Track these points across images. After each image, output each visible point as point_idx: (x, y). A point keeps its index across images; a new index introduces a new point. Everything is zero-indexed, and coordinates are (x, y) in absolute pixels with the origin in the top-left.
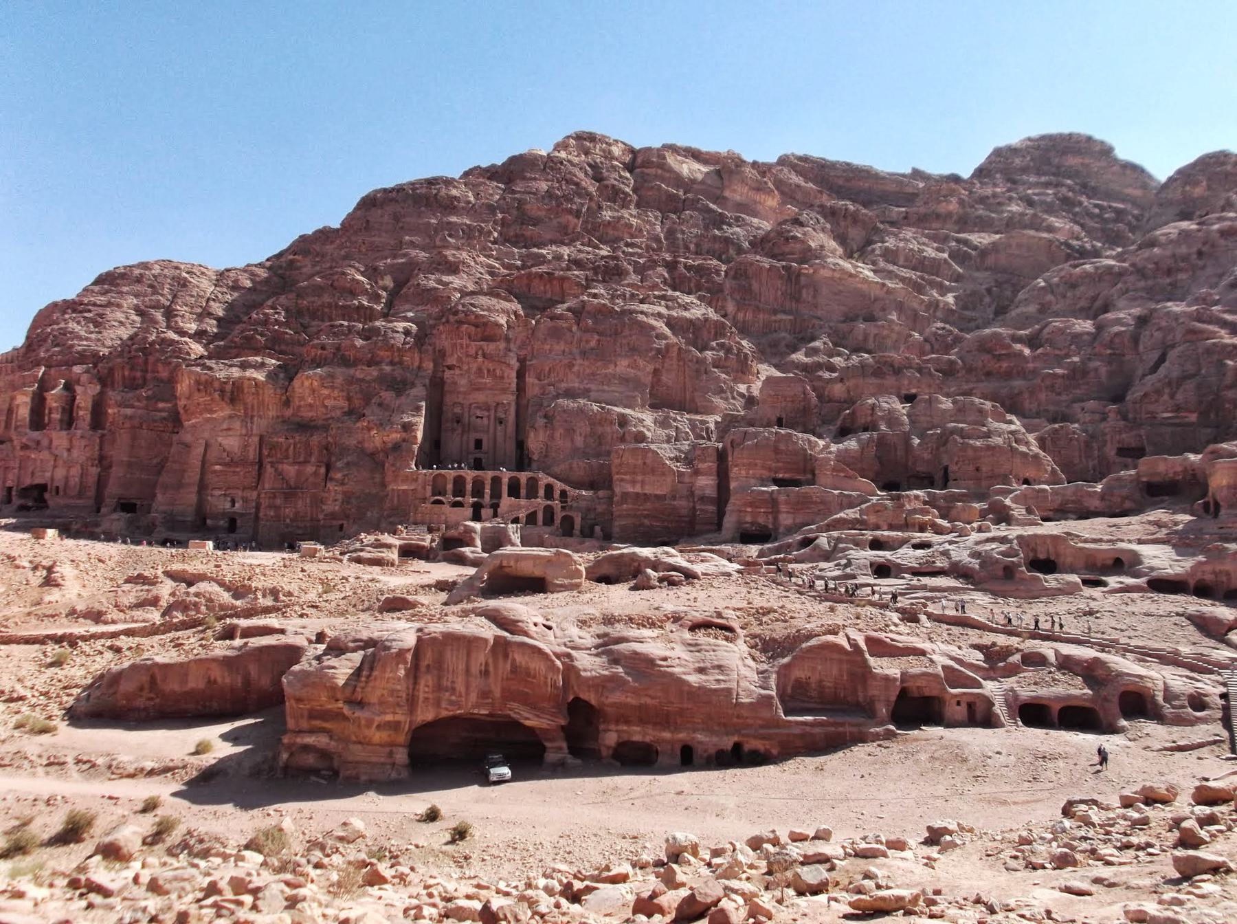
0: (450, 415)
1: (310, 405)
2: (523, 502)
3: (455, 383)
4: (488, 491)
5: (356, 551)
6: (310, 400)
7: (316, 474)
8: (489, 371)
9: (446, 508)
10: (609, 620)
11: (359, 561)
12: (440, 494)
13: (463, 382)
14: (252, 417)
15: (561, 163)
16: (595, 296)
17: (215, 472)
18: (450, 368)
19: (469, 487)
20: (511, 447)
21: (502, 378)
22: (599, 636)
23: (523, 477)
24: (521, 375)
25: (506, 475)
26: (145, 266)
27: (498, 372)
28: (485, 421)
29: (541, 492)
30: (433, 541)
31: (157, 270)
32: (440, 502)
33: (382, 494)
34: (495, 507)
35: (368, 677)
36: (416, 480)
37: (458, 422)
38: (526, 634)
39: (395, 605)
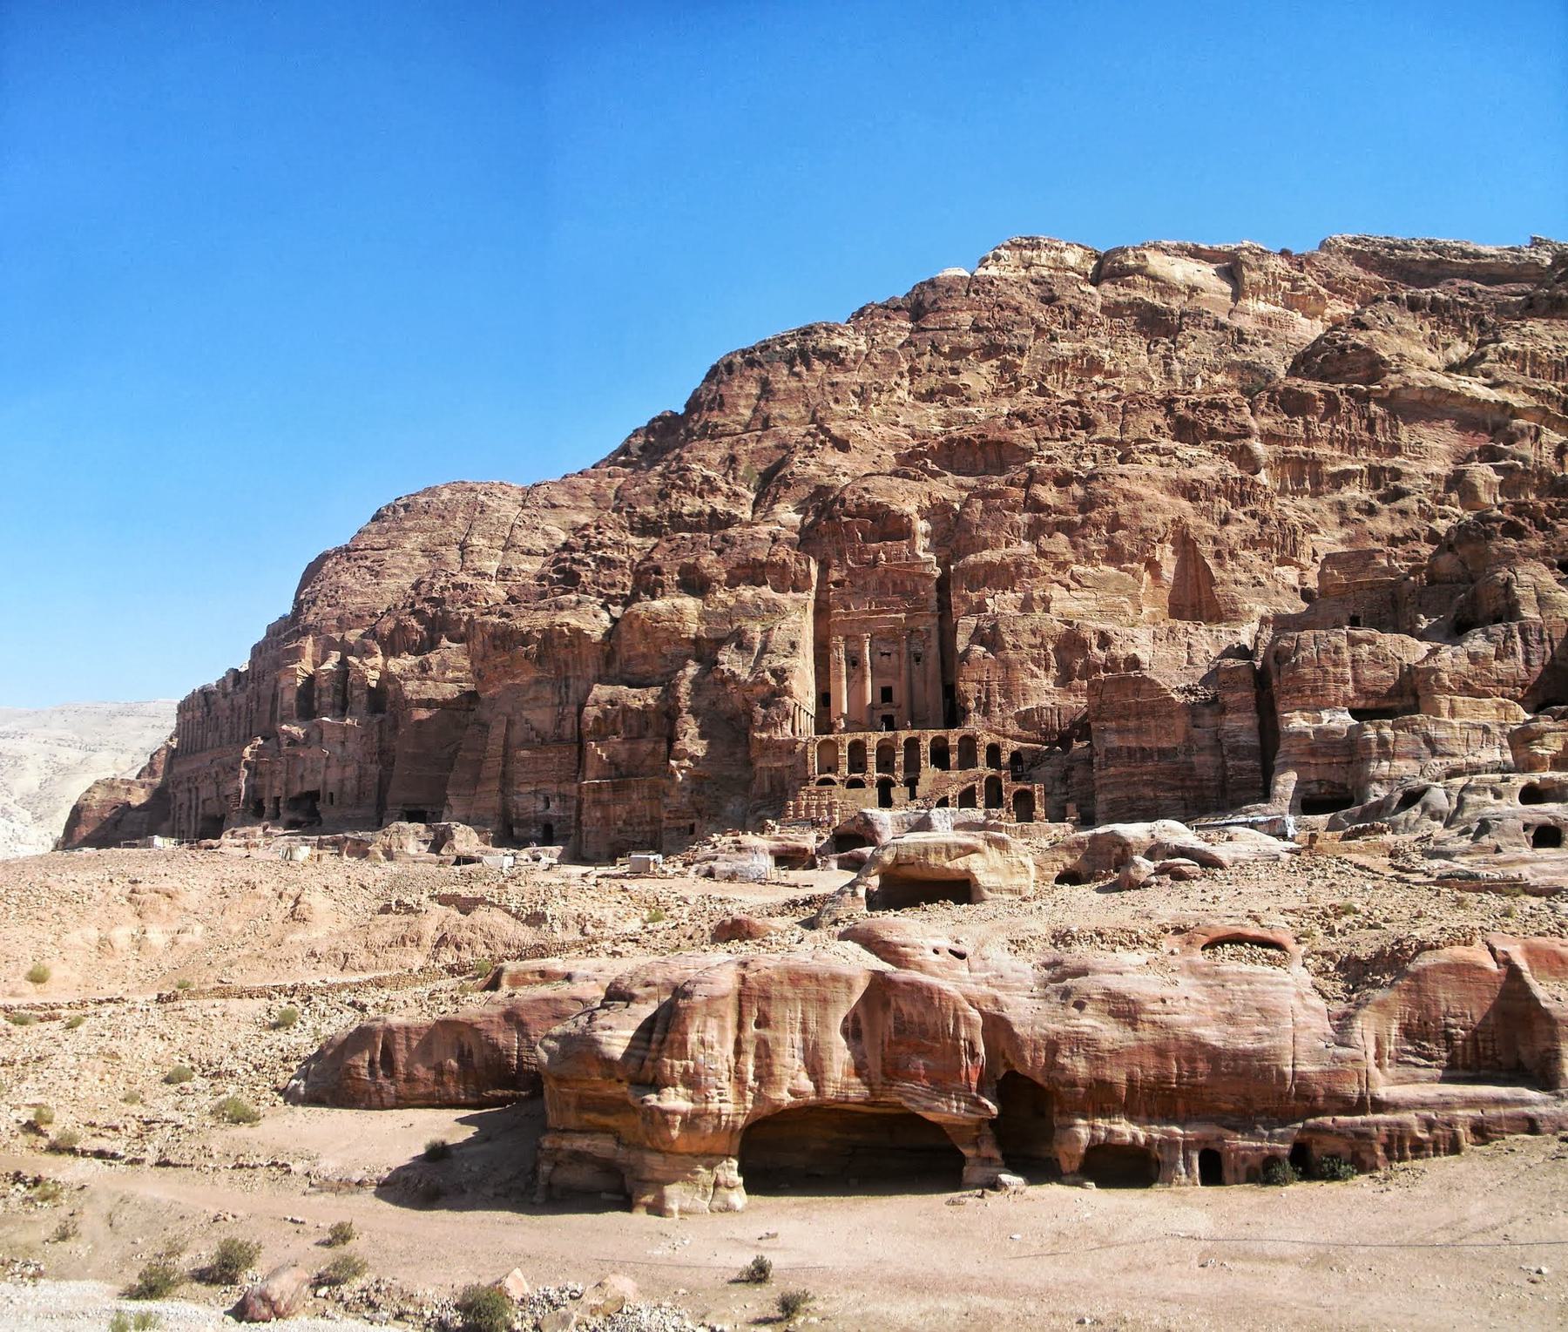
1: (644, 656)
2: (954, 774)
4: (900, 759)
5: (707, 859)
6: (642, 649)
7: (653, 753)
8: (895, 584)
9: (840, 791)
10: (1062, 938)
11: (710, 874)
12: (829, 770)
14: (567, 678)
15: (992, 283)
16: (1050, 459)
17: (523, 760)
19: (872, 760)
20: (932, 697)
22: (1047, 966)
23: (953, 737)
25: (927, 738)
26: (431, 491)
28: (894, 657)
29: (982, 756)
30: (819, 838)
31: (446, 495)
32: (830, 782)
33: (747, 776)
34: (912, 783)
35: (662, 1042)
38: (921, 967)
39: (732, 931)
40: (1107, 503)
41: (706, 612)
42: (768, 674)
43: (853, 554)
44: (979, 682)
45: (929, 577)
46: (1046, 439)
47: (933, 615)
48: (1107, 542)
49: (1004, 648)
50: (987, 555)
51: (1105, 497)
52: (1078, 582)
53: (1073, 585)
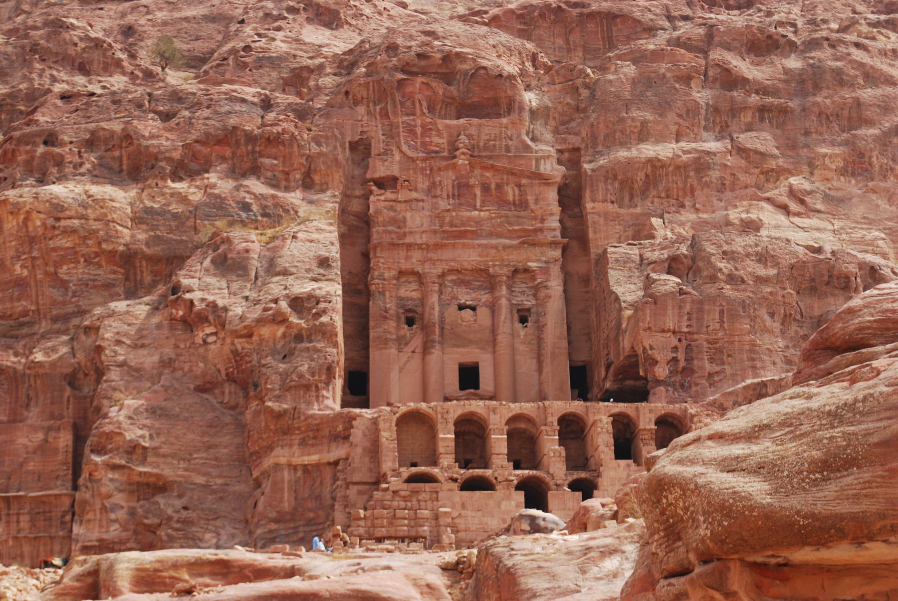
0: (391, 305)
1: (20, 283)
3: (400, 223)
7: (44, 449)
8: (486, 188)
13: (417, 221)
18: (382, 184)
21: (522, 204)
24: (571, 197)
27: (511, 193)
36: (346, 438)
37: (410, 322)
40: (842, 83)
41: (149, 211)
42: (284, 304)
43: (411, 131)
44: (674, 332)
45: (544, 180)
46: (686, 18)
47: (553, 244)
48: (846, 143)
49: (713, 279)
50: (648, 150)
51: (838, 72)
52: (802, 202)
53: (794, 206)
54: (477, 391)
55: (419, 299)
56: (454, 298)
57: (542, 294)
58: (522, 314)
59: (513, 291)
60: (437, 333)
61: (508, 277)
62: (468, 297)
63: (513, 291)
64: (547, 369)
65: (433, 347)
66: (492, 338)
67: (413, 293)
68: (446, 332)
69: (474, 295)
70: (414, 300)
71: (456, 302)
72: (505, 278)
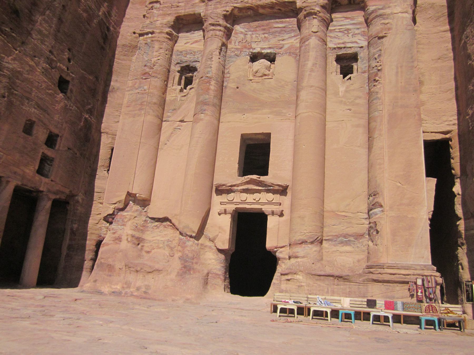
54: (263, 178)
55: (201, 51)
56: (245, 47)
57: (376, 28)
58: (345, 63)
59: (331, 31)
60: (212, 93)
61: (323, 7)
62: (265, 45)
63: (331, 31)
64: (382, 142)
65: (202, 111)
66: (295, 98)
67: (194, 45)
68: (228, 92)
69: (273, 41)
70: (193, 53)
71: (248, 52)
72: (318, 9)
